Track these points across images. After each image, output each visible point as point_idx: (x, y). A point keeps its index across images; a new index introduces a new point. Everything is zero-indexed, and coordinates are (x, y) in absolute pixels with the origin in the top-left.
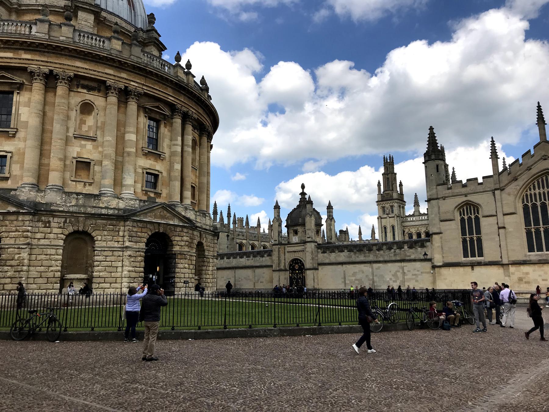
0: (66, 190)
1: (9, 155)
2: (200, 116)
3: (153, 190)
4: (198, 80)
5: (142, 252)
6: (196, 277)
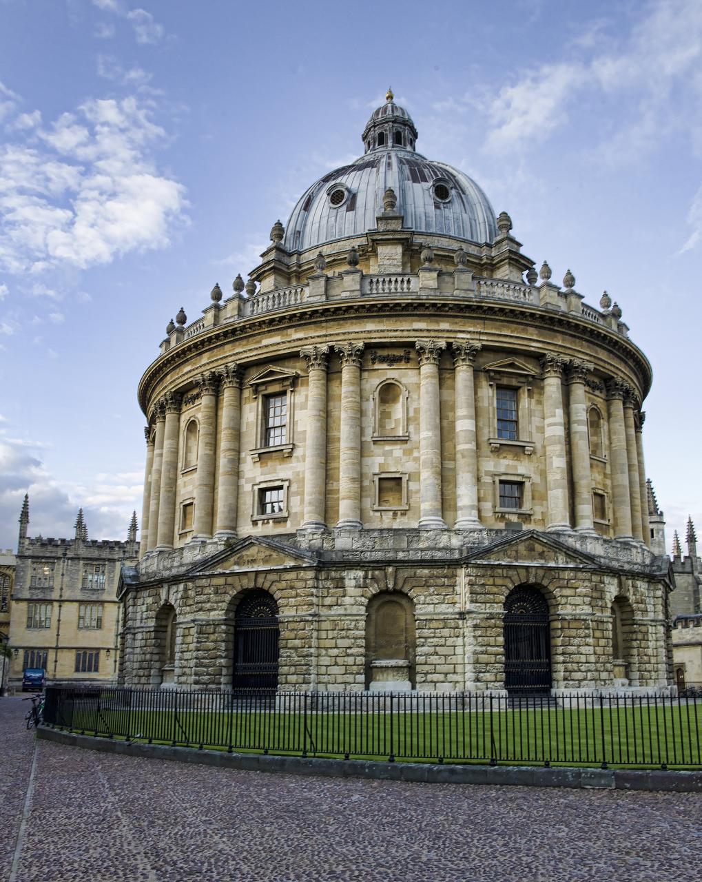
0: (367, 526)
1: (286, 484)
2: (601, 363)
3: (514, 510)
4: (594, 301)
5: (499, 618)
6: (620, 661)
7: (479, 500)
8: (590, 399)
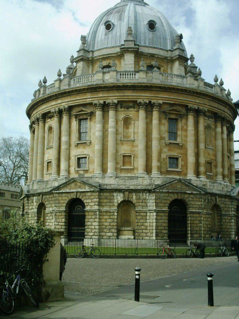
8: (124, 114)
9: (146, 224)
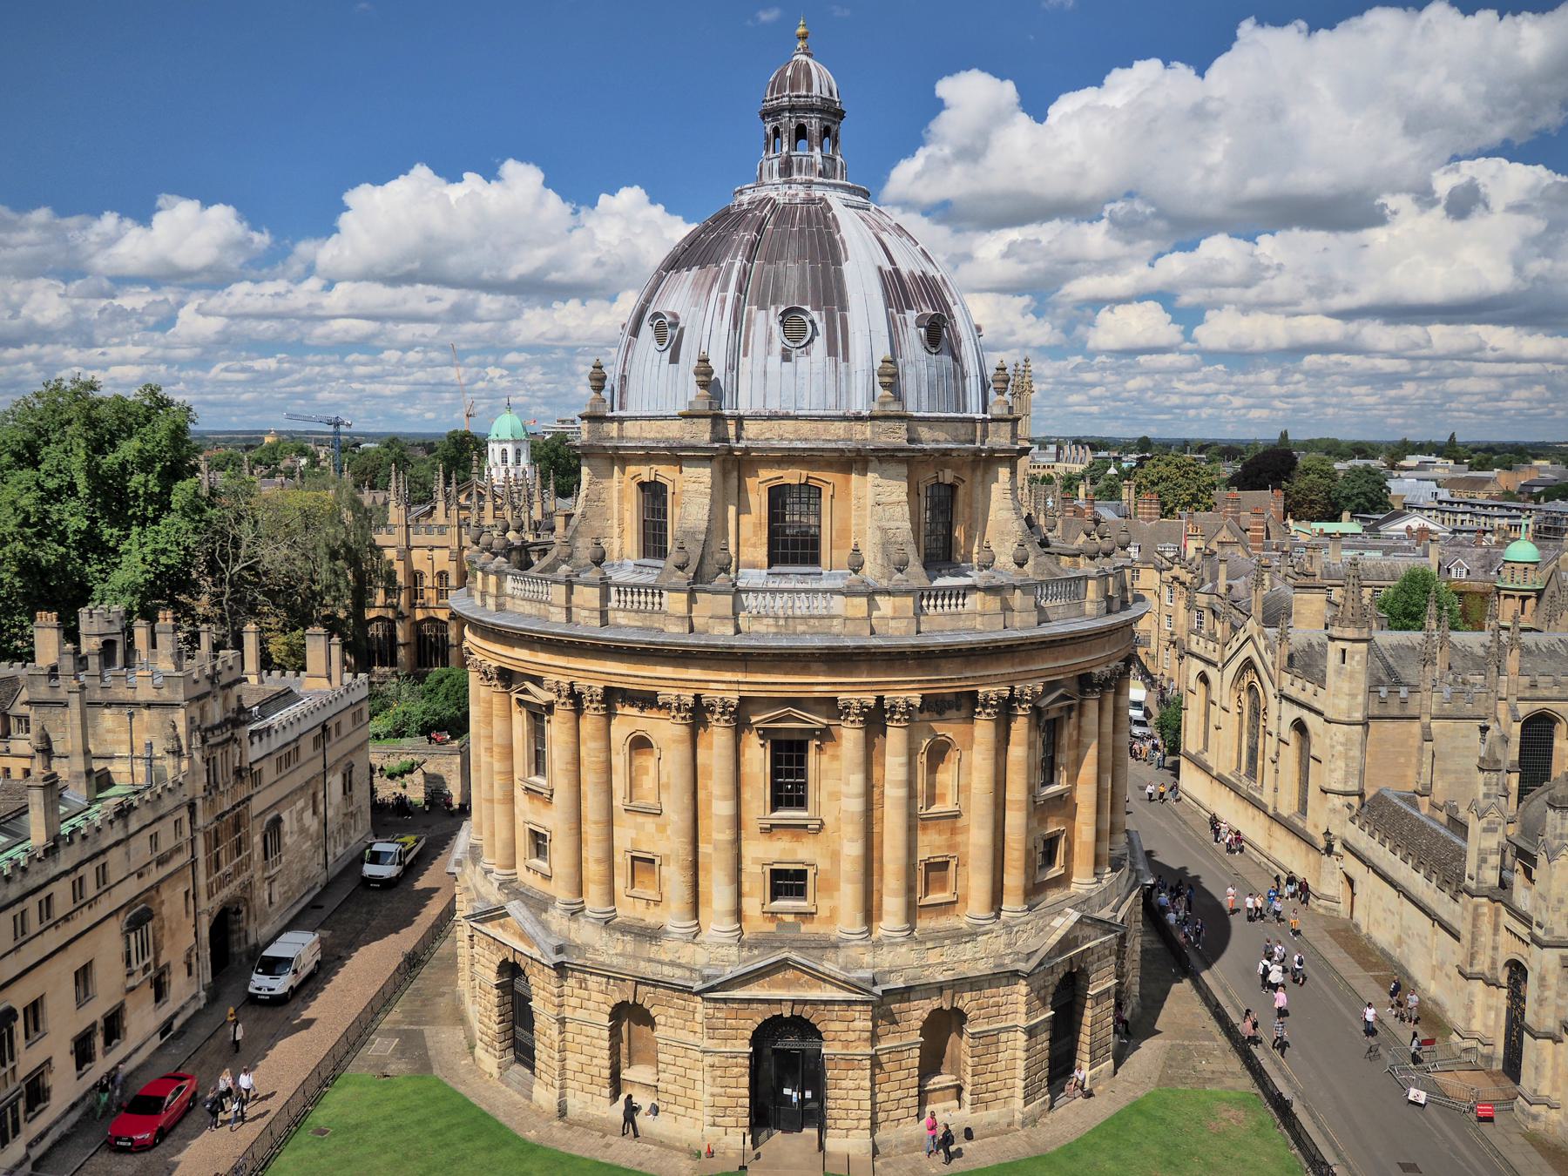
7: (739, 895)
9: (997, 1067)
